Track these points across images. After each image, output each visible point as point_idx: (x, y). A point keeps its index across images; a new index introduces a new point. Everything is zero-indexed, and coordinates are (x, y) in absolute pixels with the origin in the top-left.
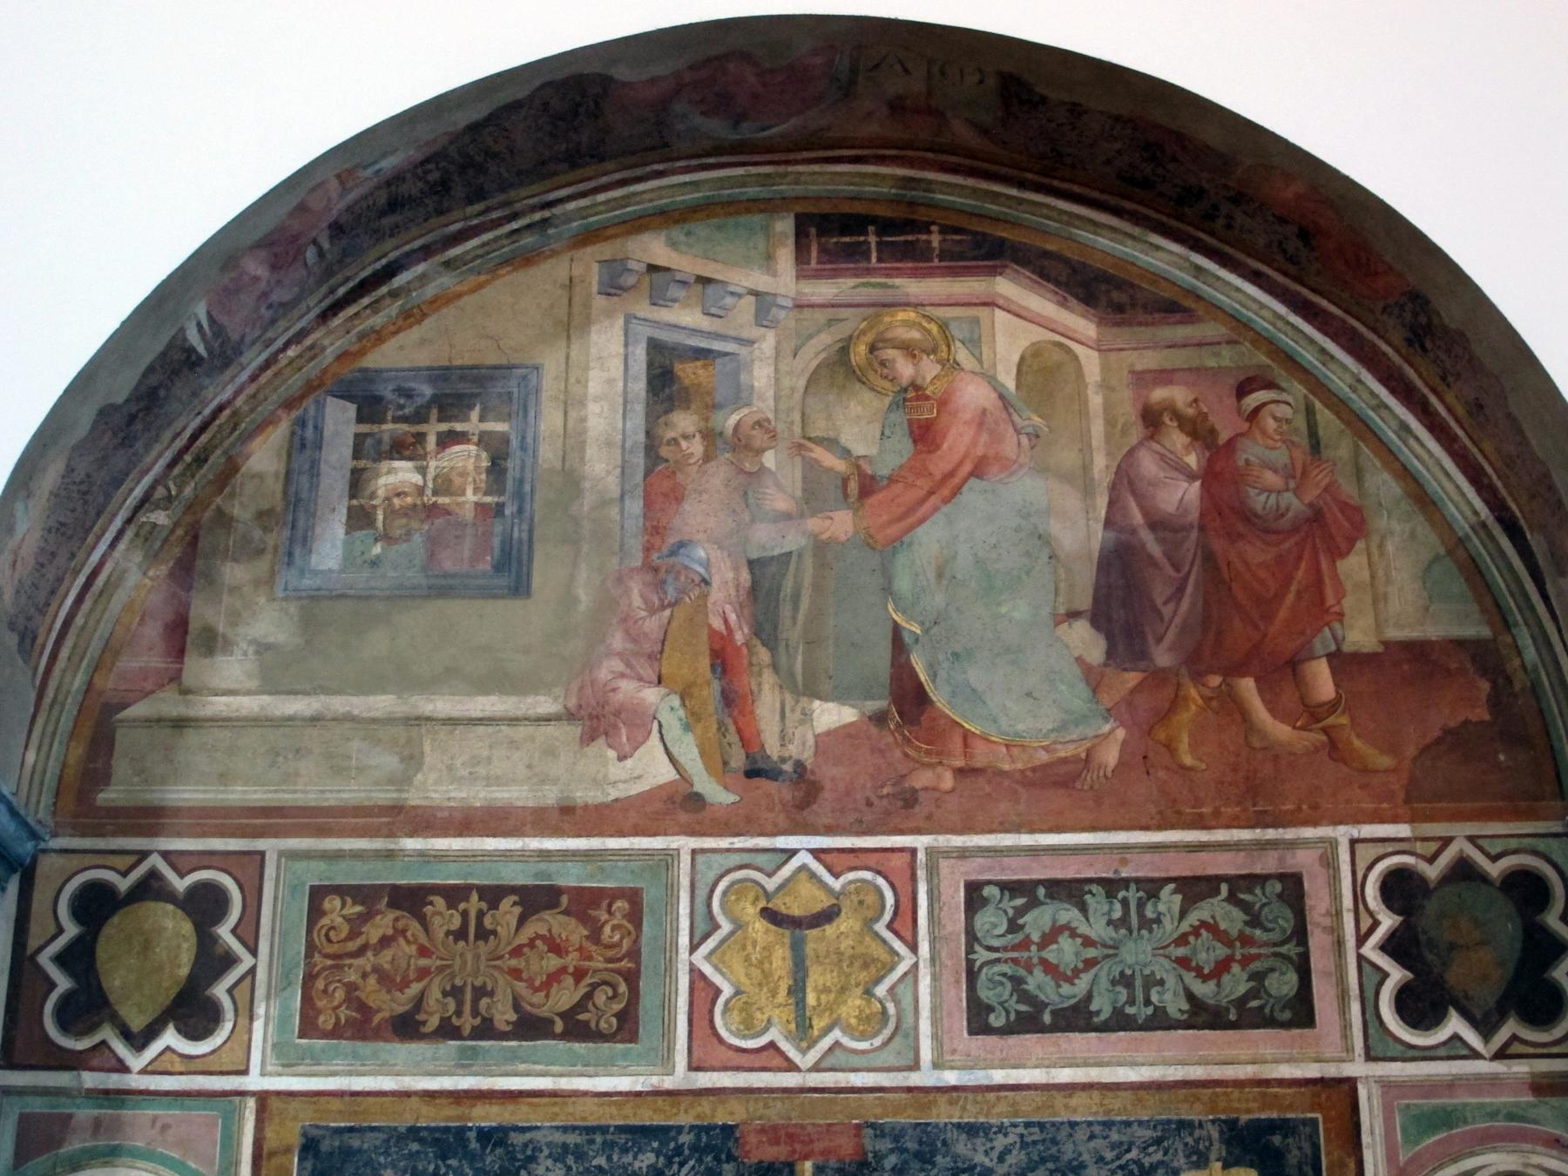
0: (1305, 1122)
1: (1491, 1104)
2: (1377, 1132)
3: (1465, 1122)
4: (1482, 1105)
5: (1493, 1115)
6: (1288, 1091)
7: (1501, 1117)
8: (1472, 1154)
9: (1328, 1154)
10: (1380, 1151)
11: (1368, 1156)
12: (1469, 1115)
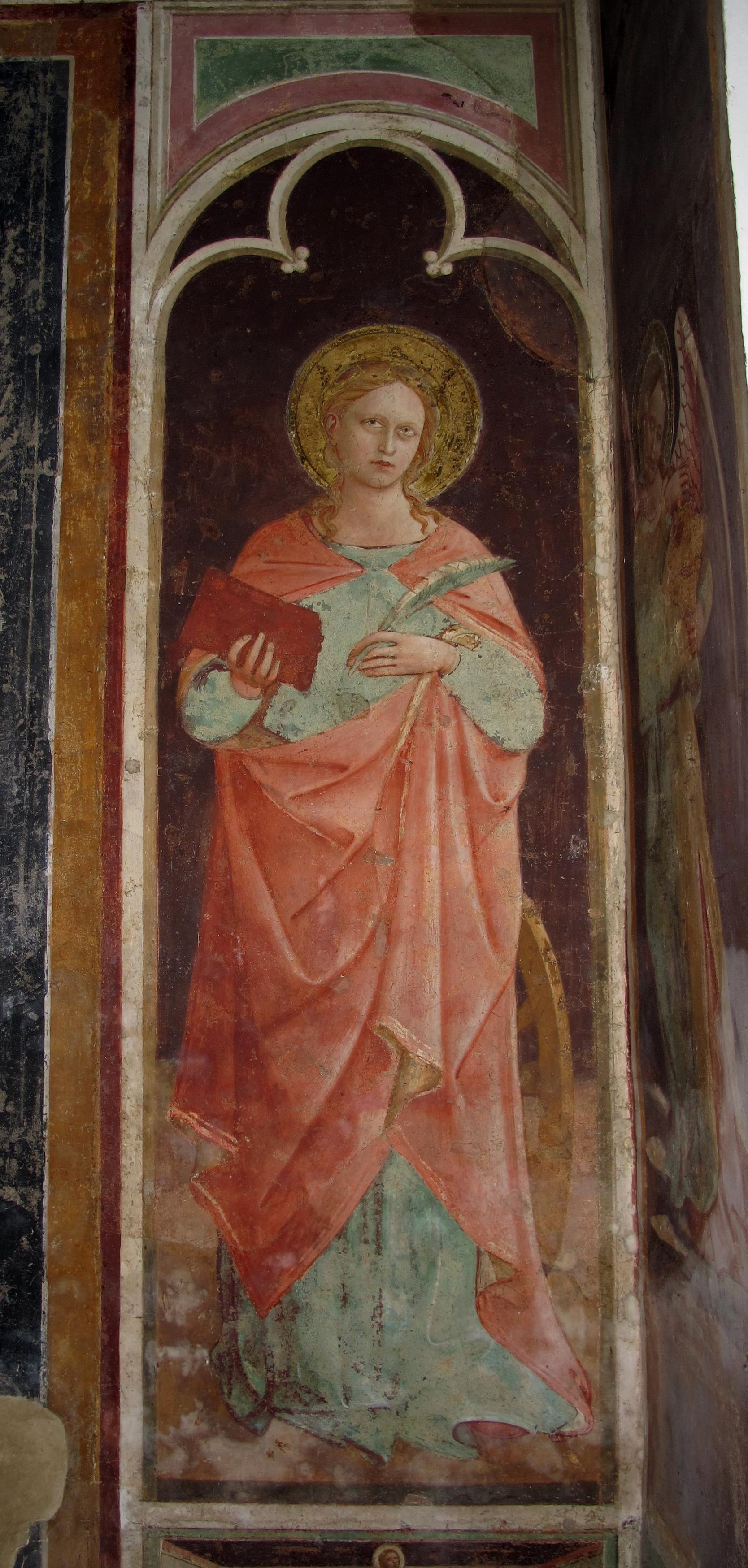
0: (45, 68)
1: (347, 42)
2: (161, 83)
3: (303, 67)
4: (333, 44)
5: (349, 59)
6: (29, 23)
7: (362, 60)
8: (310, 116)
9: (76, 114)
10: (163, 109)
11: (142, 116)
12: (309, 58)
